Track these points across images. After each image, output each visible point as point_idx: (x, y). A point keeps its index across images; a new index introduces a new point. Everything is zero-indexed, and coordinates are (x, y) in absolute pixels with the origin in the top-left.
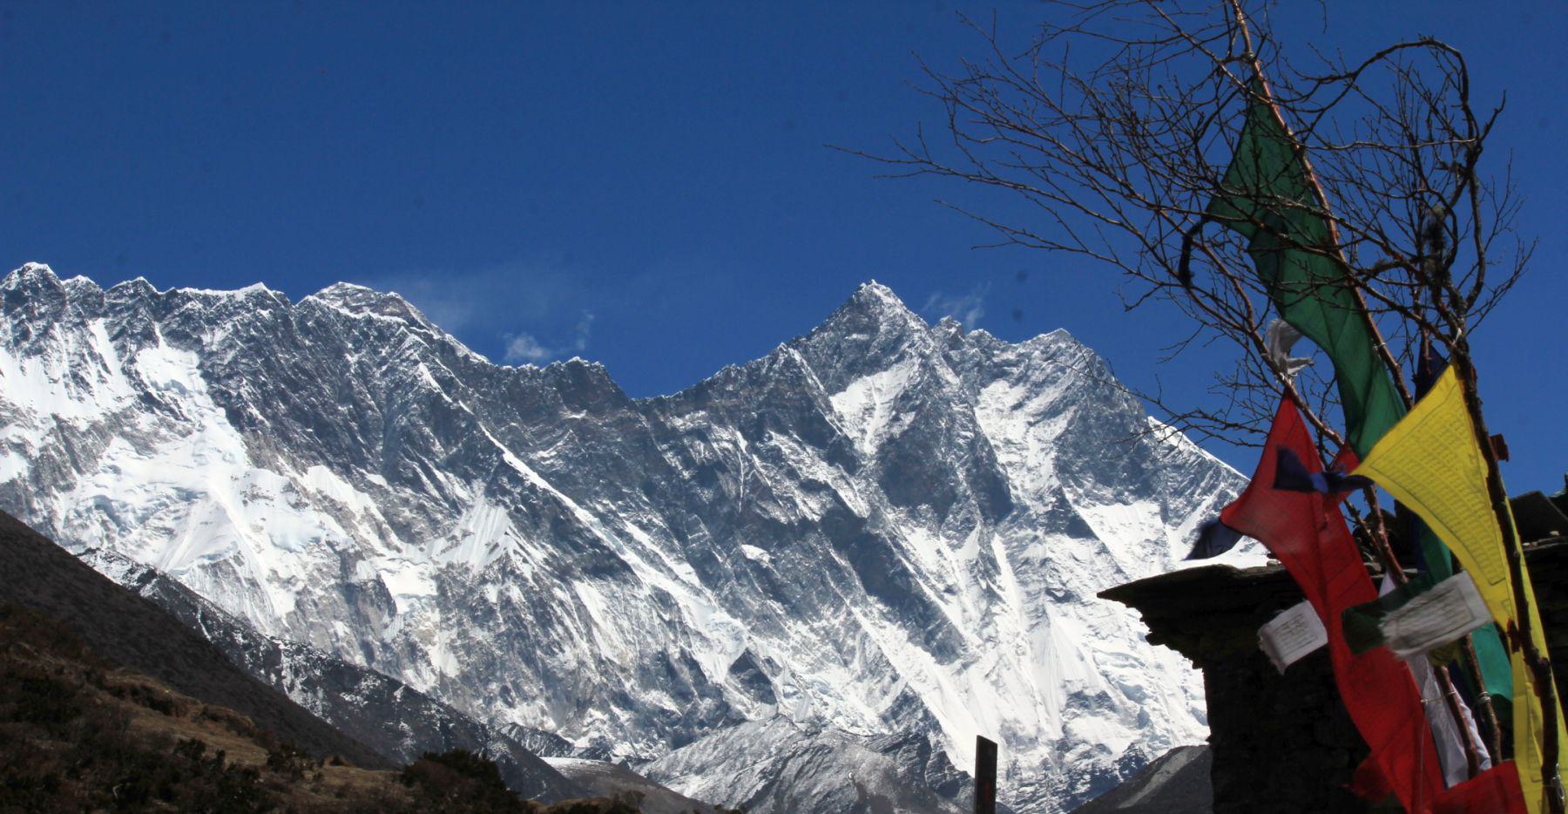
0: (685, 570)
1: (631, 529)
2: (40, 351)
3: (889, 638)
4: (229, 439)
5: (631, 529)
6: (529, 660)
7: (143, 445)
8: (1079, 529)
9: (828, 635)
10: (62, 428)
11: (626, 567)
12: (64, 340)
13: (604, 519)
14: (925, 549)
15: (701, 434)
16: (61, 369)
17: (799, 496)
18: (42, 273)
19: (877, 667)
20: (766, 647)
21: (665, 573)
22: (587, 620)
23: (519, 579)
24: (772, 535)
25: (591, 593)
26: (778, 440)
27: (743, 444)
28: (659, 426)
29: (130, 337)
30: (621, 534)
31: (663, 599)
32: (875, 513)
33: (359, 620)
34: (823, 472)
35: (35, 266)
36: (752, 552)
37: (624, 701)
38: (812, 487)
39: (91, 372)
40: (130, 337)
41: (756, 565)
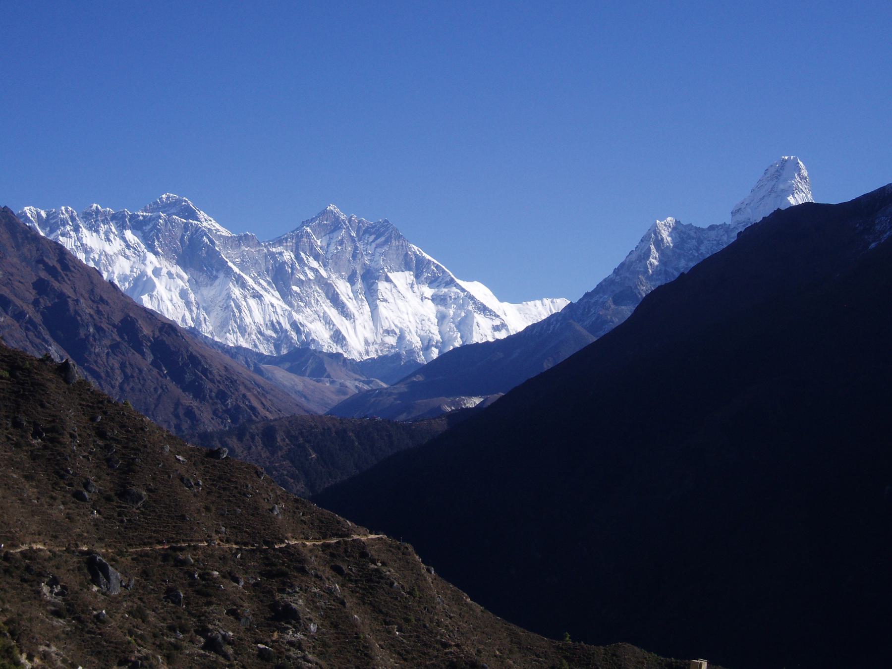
0: (277, 294)
1: (262, 281)
2: (97, 231)
3: (333, 313)
4: (150, 256)
5: (262, 281)
6: (236, 322)
7: (127, 258)
8: (388, 280)
9: (316, 312)
10: (104, 253)
11: (261, 296)
12: (103, 228)
13: (254, 279)
14: (343, 288)
15: (281, 254)
16: (103, 236)
17: (308, 272)
18: (97, 207)
19: (328, 322)
20: (297, 317)
21: (272, 297)
22: (250, 311)
23: (233, 300)
24: (300, 283)
25: (252, 302)
26: (303, 255)
27: (293, 256)
28: (268, 250)
29: (122, 227)
30: (260, 284)
31: (273, 306)
32: (330, 277)
33: (191, 311)
34: (314, 264)
35: (95, 205)
36: (295, 288)
37: (260, 333)
38: (312, 269)
39: (112, 236)
40: (122, 227)
41: (296, 292)
